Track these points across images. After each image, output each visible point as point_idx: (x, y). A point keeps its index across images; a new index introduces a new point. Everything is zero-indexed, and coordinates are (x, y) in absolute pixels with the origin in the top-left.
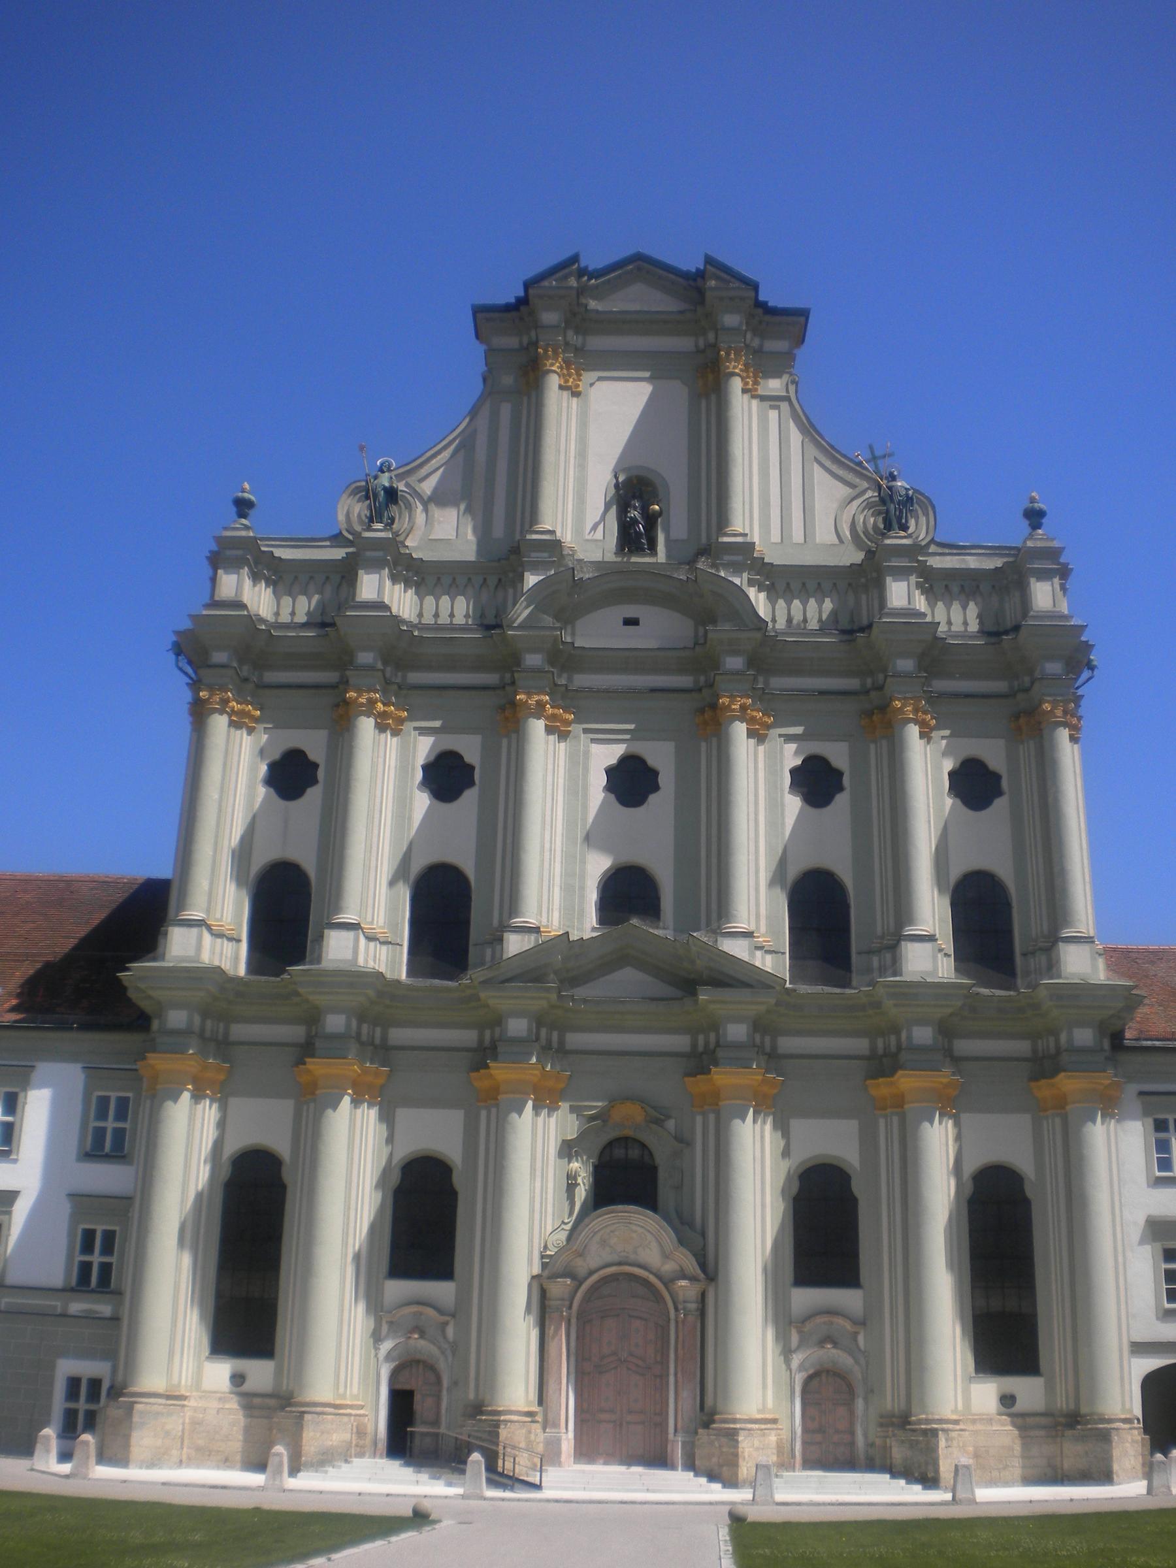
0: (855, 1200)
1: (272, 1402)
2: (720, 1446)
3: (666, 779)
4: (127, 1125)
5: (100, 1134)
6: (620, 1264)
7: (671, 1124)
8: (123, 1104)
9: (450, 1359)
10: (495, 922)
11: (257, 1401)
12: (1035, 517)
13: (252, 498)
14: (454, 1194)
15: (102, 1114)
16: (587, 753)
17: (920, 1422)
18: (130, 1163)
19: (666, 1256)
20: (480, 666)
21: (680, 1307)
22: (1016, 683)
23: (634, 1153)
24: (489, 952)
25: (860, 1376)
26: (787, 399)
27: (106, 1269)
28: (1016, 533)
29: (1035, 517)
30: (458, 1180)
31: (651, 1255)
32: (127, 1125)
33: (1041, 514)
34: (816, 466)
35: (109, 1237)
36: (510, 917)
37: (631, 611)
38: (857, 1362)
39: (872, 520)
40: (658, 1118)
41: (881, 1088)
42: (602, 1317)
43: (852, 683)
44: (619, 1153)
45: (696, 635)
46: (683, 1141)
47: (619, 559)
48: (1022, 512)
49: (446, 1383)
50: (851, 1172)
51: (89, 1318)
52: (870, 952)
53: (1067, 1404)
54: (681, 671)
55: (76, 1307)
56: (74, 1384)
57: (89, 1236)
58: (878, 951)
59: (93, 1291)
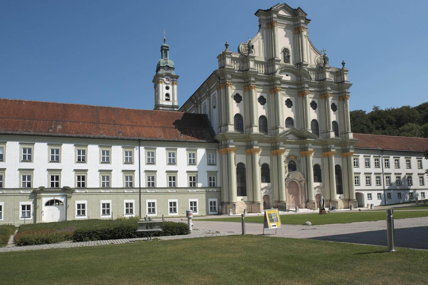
0: (321, 170)
1: (248, 202)
2: (312, 205)
3: (294, 103)
4: (209, 159)
5: (210, 161)
6: (293, 179)
7: (298, 159)
9: (271, 194)
10: (272, 126)
11: (246, 202)
12: (343, 64)
13: (229, 44)
14: (269, 169)
15: (210, 157)
16: (282, 98)
17: (334, 200)
18: (216, 166)
19: (300, 178)
20: (266, 81)
21: (302, 185)
22: (339, 92)
23: (293, 163)
24: (272, 131)
25: (322, 195)
26: (307, 36)
27: (214, 183)
28: (341, 67)
29: (343, 64)
30: (270, 167)
31: (298, 178)
32: (209, 159)
33: (345, 64)
34: (312, 50)
35: (214, 178)
36: (278, 126)
37: (287, 73)
38: (322, 193)
39: (320, 60)
40: (296, 158)
41: (326, 153)
42: (290, 187)
43: (318, 89)
44: (291, 163)
45: (297, 79)
46: (300, 162)
47: (285, 64)
48: (341, 63)
49: (271, 198)
50: (320, 166)
51: (212, 191)
52: (322, 133)
53: (348, 198)
54: (295, 85)
55: (210, 190)
56: (211, 202)
57: (210, 178)
58: (324, 133)
59: (212, 187)
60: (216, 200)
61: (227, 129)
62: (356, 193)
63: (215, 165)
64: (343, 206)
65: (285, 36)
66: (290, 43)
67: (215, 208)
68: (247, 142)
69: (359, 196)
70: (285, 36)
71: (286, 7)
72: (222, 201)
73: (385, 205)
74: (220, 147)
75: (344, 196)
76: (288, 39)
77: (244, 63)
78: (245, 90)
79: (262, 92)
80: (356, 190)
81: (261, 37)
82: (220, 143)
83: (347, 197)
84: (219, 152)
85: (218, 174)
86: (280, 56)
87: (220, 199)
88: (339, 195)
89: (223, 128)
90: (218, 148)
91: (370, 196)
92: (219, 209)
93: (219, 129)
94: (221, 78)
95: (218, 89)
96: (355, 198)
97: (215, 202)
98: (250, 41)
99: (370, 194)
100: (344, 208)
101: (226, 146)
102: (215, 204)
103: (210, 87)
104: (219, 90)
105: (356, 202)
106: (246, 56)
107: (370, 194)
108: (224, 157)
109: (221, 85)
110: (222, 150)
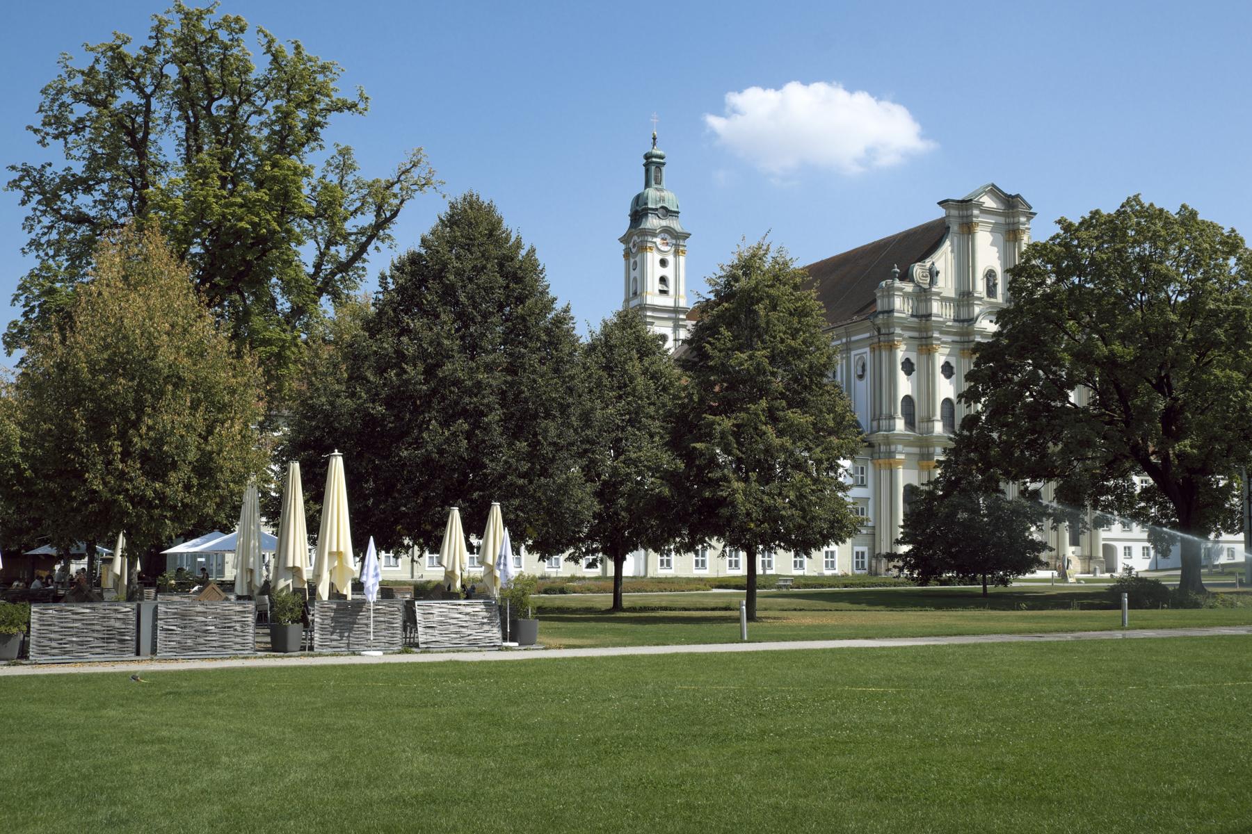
8: (862, 468)
20: (955, 334)
56: (857, 553)
60: (865, 549)
61: (891, 428)
62: (1104, 545)
63: (865, 486)
64: (1079, 569)
65: (992, 244)
66: (999, 258)
67: (863, 563)
68: (921, 447)
69: (1109, 550)
70: (992, 244)
71: (994, 191)
72: (877, 552)
73: (1157, 570)
74: (876, 456)
75: (1082, 550)
76: (996, 249)
77: (921, 301)
78: (920, 352)
79: (948, 355)
80: (1104, 539)
81: (950, 249)
82: (877, 448)
83: (1087, 553)
84: (874, 465)
85: (871, 503)
86: (981, 287)
87: (873, 548)
88: (1073, 548)
89: (884, 423)
90: (873, 458)
91: (1128, 551)
92: (870, 566)
93: (875, 423)
94: (883, 331)
95: (873, 350)
96: (1101, 554)
97: (863, 553)
98: (933, 264)
99: (1129, 548)
100: (1082, 573)
101: (890, 455)
102: (863, 557)
103: (850, 336)
104: (877, 352)
105: (1102, 562)
106: (925, 290)
107: (1129, 548)
108: (885, 474)
109: (882, 344)
110: (881, 461)
